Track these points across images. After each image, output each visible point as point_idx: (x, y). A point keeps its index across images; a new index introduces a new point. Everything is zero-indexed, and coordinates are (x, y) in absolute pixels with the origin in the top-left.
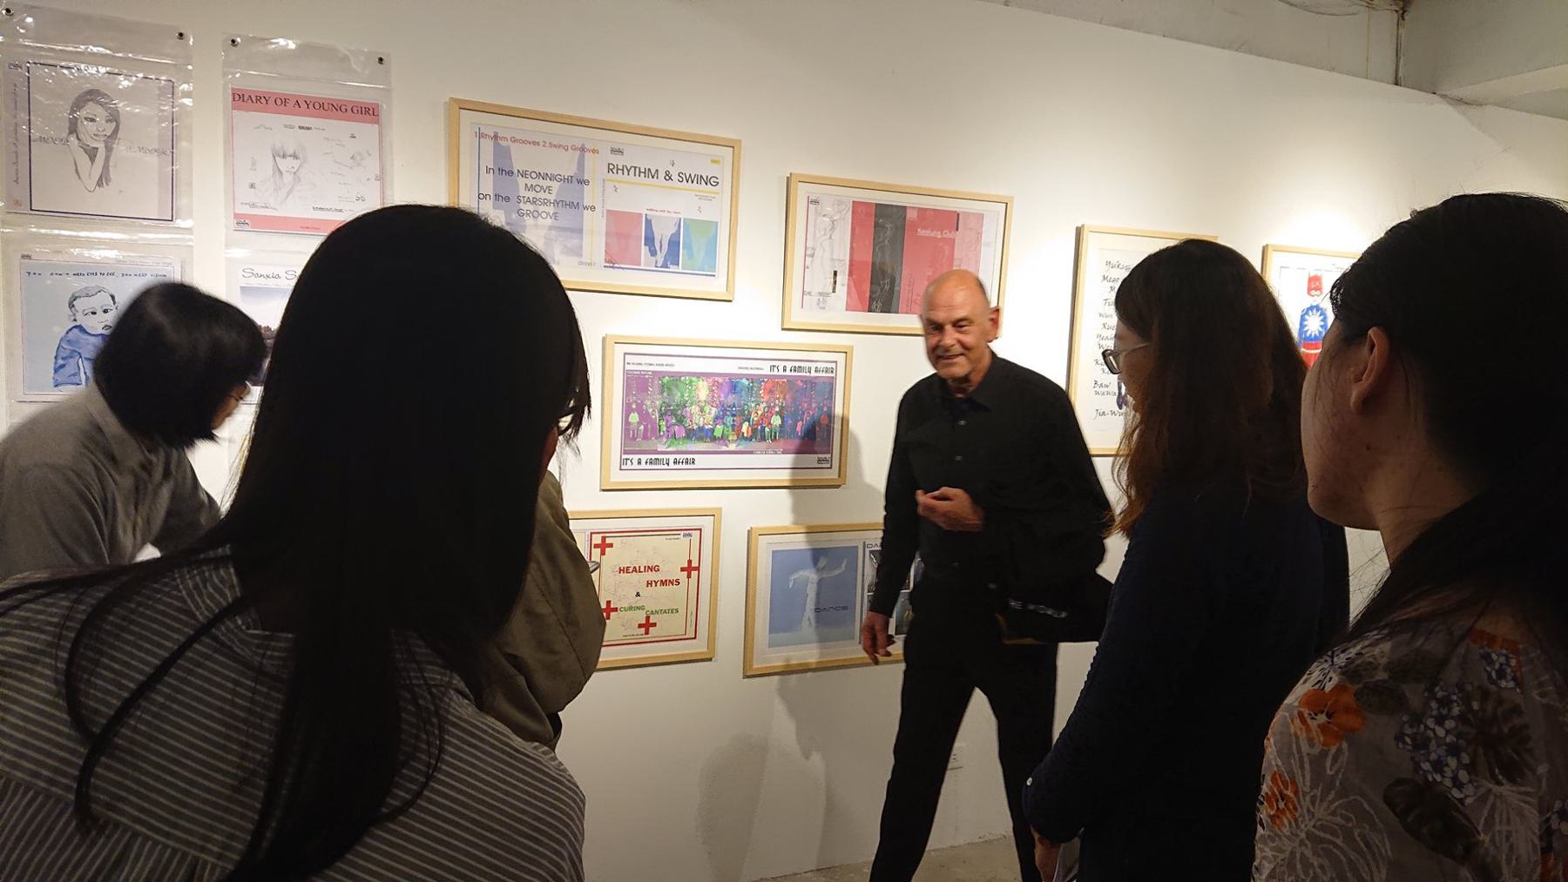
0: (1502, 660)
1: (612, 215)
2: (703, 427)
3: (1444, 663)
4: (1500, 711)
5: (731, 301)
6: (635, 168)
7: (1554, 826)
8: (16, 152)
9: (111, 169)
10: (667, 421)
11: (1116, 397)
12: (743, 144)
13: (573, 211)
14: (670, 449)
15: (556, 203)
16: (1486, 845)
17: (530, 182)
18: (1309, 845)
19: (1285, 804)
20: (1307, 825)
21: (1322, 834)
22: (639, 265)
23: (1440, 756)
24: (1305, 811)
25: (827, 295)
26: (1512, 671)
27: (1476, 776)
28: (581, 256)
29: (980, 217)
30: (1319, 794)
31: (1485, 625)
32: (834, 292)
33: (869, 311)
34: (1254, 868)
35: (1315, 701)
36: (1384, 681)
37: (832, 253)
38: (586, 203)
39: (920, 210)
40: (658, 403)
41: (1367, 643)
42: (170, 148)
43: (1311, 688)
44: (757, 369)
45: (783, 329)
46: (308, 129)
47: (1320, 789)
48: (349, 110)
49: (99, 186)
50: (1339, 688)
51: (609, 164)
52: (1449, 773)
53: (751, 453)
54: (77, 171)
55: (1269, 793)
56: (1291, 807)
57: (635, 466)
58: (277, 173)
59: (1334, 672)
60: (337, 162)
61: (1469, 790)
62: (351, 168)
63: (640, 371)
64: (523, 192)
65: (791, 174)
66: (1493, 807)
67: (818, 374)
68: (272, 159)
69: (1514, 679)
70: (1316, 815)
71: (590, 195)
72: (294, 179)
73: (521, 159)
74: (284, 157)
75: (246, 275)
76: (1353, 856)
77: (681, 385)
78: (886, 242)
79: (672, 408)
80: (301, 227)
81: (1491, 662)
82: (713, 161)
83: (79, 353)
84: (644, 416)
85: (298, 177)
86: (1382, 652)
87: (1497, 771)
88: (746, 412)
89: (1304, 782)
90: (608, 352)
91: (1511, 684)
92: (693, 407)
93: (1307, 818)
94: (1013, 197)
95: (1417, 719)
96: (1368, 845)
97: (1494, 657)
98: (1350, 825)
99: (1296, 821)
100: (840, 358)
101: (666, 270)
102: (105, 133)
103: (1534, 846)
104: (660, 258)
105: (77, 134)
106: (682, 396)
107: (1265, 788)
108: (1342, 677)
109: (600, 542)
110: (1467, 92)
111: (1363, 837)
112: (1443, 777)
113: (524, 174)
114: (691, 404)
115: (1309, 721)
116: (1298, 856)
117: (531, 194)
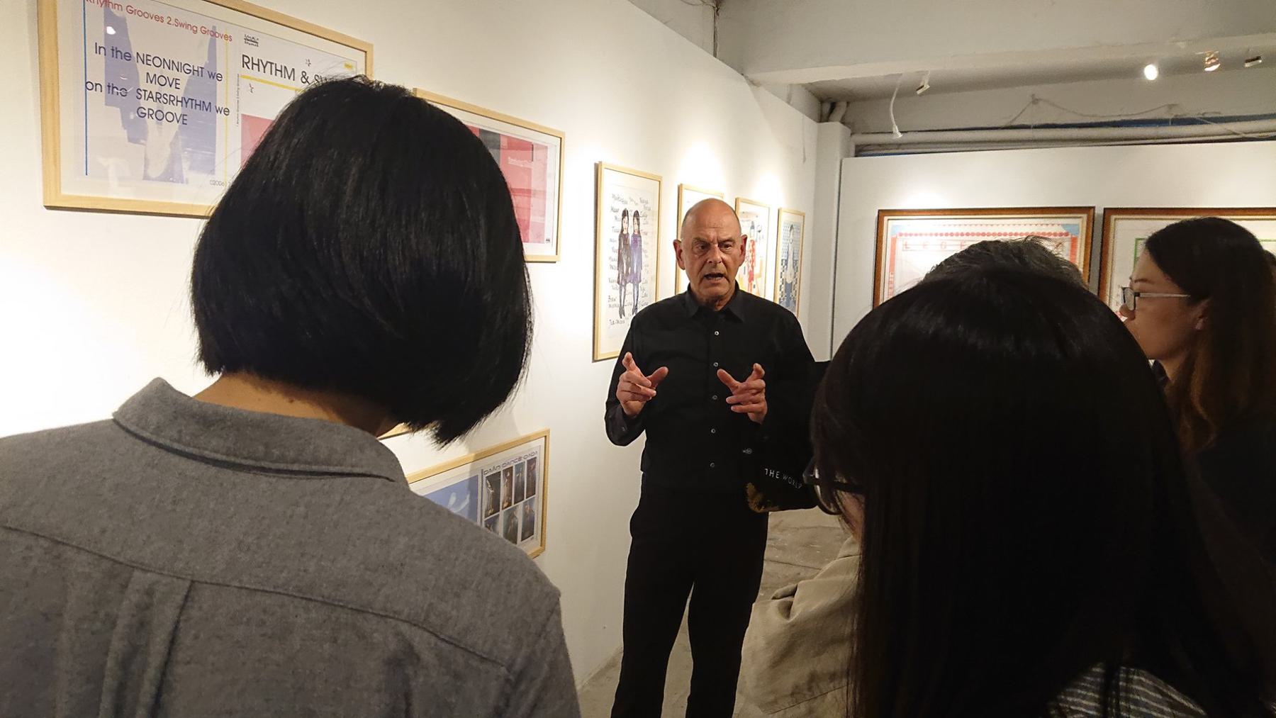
6: (271, 63)
12: (375, 48)
13: (204, 113)
15: (184, 101)
17: (153, 71)
38: (220, 105)
51: (244, 56)
64: (143, 85)
71: (224, 94)
94: (564, 133)
110: (757, 76)
113: (146, 60)
117: (154, 88)
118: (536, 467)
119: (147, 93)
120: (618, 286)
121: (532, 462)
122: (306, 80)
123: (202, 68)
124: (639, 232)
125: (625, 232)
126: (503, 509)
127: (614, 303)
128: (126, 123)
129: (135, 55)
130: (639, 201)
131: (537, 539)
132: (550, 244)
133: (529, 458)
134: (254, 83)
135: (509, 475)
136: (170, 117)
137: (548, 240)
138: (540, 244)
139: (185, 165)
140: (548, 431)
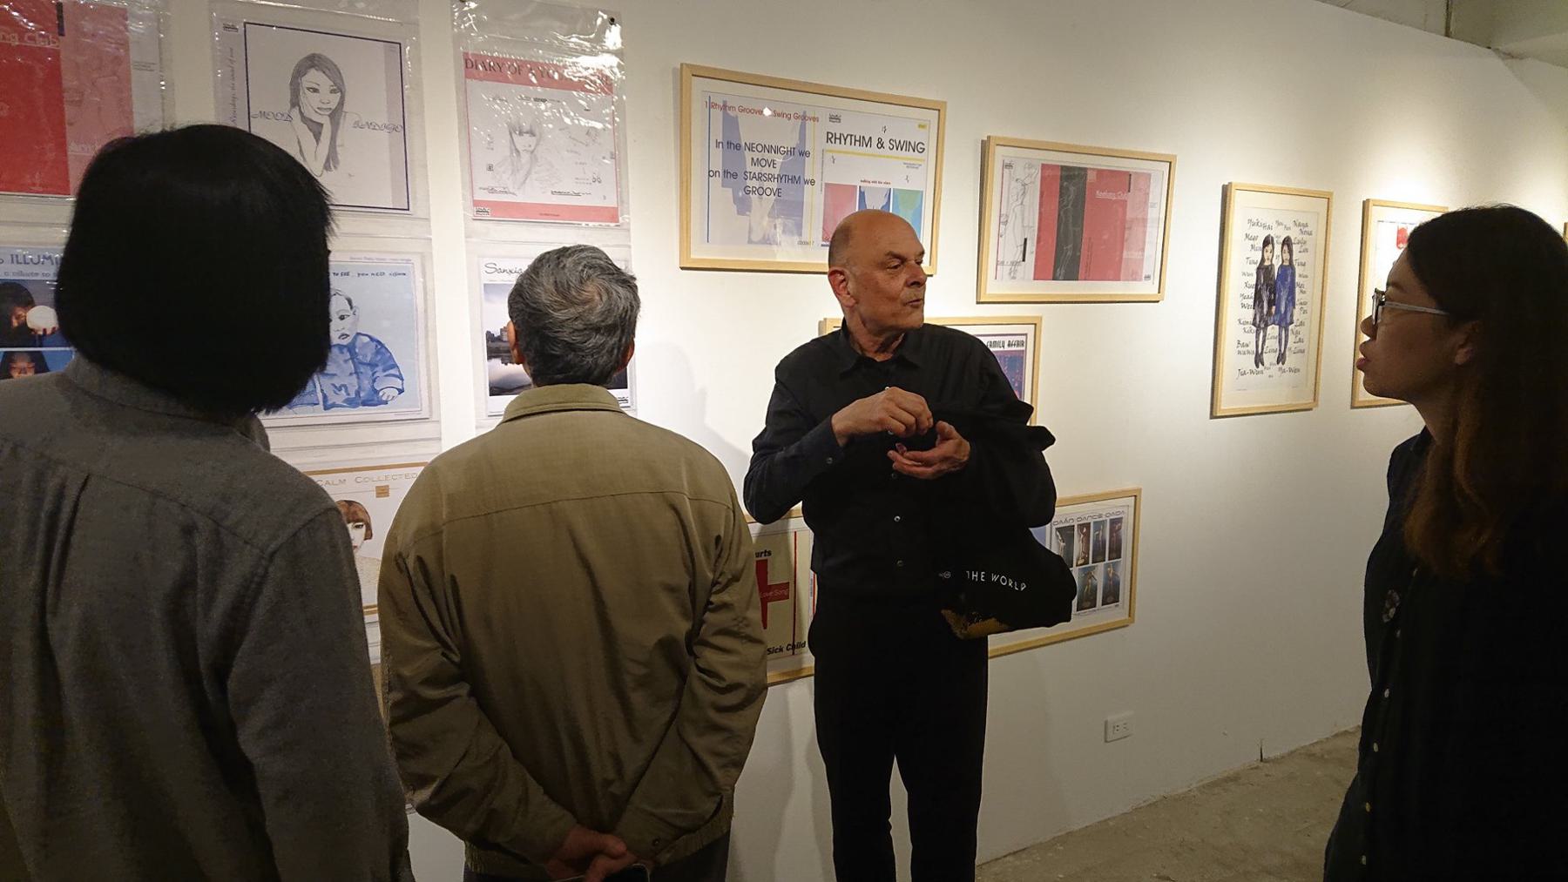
6: (851, 136)
9: (338, 149)
11: (1254, 356)
12: (948, 105)
15: (780, 178)
17: (756, 155)
25: (1015, 264)
37: (1023, 219)
38: (807, 177)
45: (978, 303)
49: (327, 170)
60: (574, 139)
62: (587, 145)
65: (989, 137)
67: (1011, 349)
71: (811, 169)
72: (531, 158)
74: (521, 133)
75: (489, 270)
78: (1069, 207)
80: (541, 214)
82: (920, 126)
85: (535, 156)
94: (1176, 156)
102: (328, 106)
105: (300, 109)
117: (757, 169)
118: (1123, 528)
120: (1254, 328)
121: (1116, 523)
124: (1291, 261)
125: (1267, 263)
126: (1077, 565)
127: (1245, 349)
128: (736, 200)
129: (743, 145)
130: (1290, 224)
131: (1123, 608)
133: (1112, 517)
135: (1085, 530)
136: (768, 192)
137: (1148, 277)
140: (1140, 490)
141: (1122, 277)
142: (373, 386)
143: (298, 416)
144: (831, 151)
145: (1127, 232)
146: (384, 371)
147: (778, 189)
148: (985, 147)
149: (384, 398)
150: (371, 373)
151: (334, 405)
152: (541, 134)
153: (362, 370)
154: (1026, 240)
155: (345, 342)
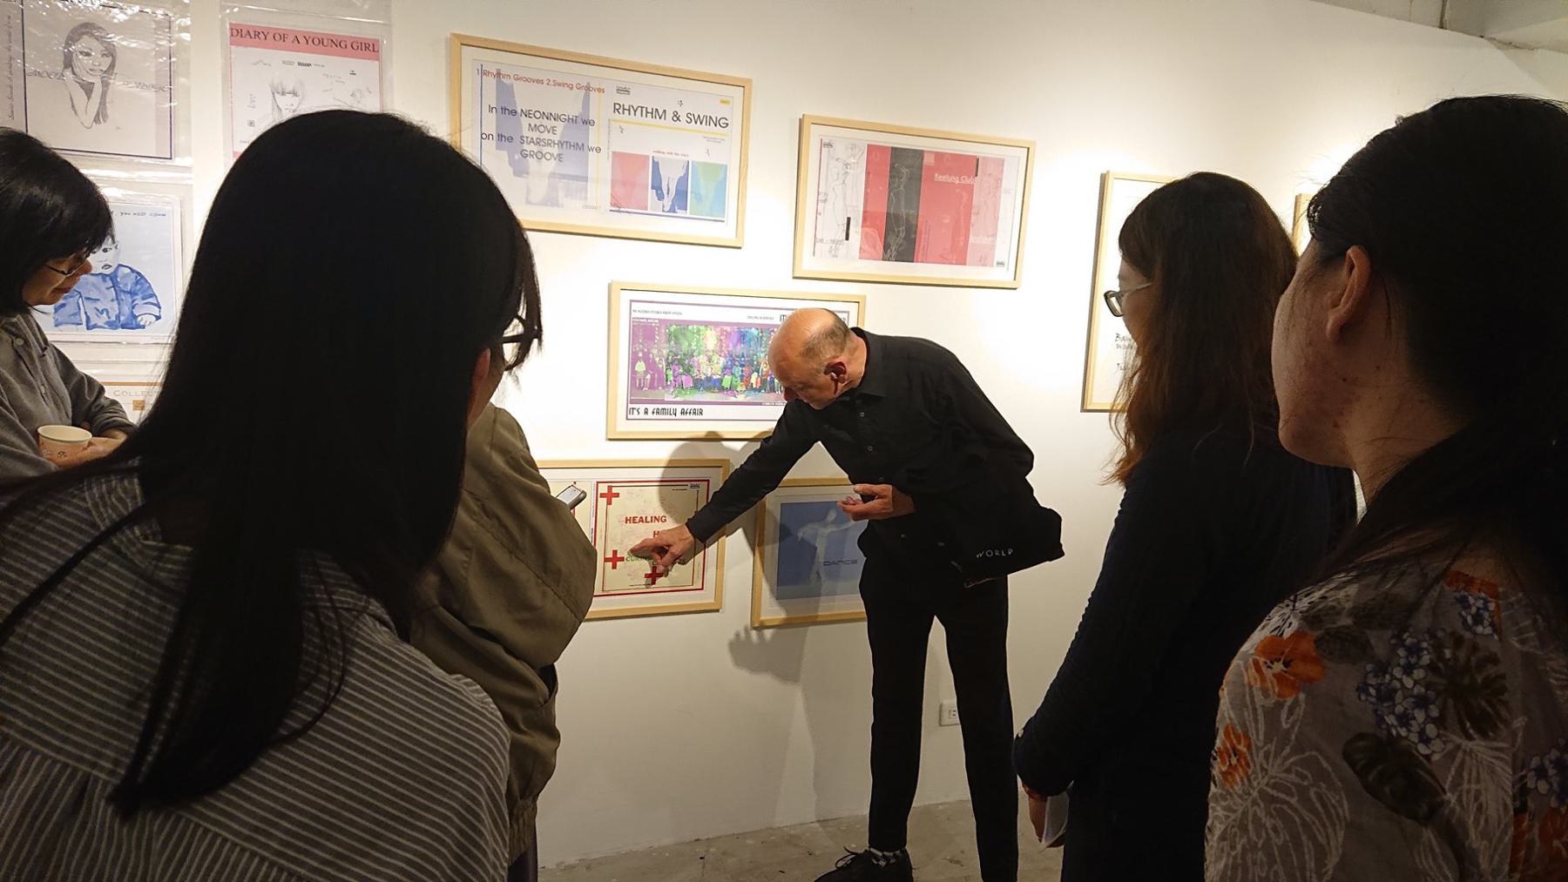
0: (1480, 604)
1: (620, 159)
2: (711, 377)
3: (1413, 608)
4: (1473, 659)
5: (740, 248)
6: (642, 107)
7: (1531, 784)
8: (11, 87)
9: (107, 105)
10: (674, 371)
14: (678, 399)
15: (561, 144)
16: (1452, 805)
18: (1262, 805)
19: (1238, 760)
20: (1260, 782)
21: (1275, 793)
22: (646, 209)
23: (1406, 709)
24: (1258, 767)
26: (1490, 616)
27: (1446, 729)
28: (586, 198)
29: (1000, 163)
30: (1273, 749)
31: (1464, 566)
32: (847, 239)
33: (883, 260)
34: (1207, 831)
35: (1272, 650)
36: (1347, 627)
37: (845, 199)
39: (937, 154)
40: (665, 352)
41: (1332, 585)
42: (167, 84)
43: (1268, 634)
44: (764, 318)
46: (309, 65)
47: (1274, 743)
48: (349, 46)
50: (1298, 635)
52: (1415, 728)
53: (760, 404)
54: (73, 106)
55: (1222, 748)
56: (1243, 763)
57: (642, 415)
58: (276, 109)
59: (1295, 617)
61: (1437, 745)
63: (647, 319)
64: (526, 133)
65: (803, 115)
66: (1462, 764)
68: (271, 97)
69: (1492, 625)
70: (1270, 773)
71: (595, 137)
73: (524, 98)
74: (283, 94)
76: (1308, 817)
77: (689, 334)
78: (902, 188)
79: (679, 357)
81: (1467, 607)
82: (722, 102)
83: (79, 293)
84: (651, 365)
86: (1348, 596)
87: (1468, 725)
88: (755, 363)
89: (1258, 736)
90: (613, 296)
91: (1488, 630)
92: (701, 356)
93: (1260, 776)
94: (1034, 143)
95: (1382, 668)
96: (1324, 806)
97: (1471, 601)
98: (1305, 783)
99: (1249, 780)
100: (853, 308)
101: (675, 215)
103: (1505, 805)
104: (667, 202)
106: (690, 345)
107: (1218, 743)
108: (1302, 621)
109: (606, 491)
111: (1320, 797)
112: (1409, 731)
113: (527, 114)
114: (699, 354)
115: (1264, 669)
116: (1250, 818)
117: (535, 135)
119: (529, 139)
122: (678, 118)
123: (576, 117)
128: (512, 162)
132: (1000, 269)
134: (622, 124)
136: (548, 156)
137: (1001, 264)
138: (984, 268)
139: (561, 194)
141: (968, 261)
142: (132, 312)
143: (78, 333)
144: (619, 121)
145: (973, 218)
146: (143, 299)
147: (559, 155)
148: (801, 121)
149: (142, 323)
150: (130, 300)
151: (95, 326)
152: (303, 97)
153: (123, 297)
154: (849, 219)
155: (108, 272)
